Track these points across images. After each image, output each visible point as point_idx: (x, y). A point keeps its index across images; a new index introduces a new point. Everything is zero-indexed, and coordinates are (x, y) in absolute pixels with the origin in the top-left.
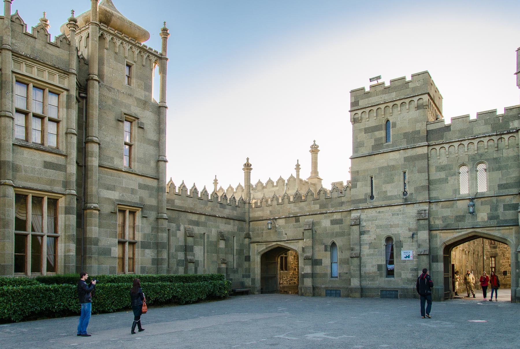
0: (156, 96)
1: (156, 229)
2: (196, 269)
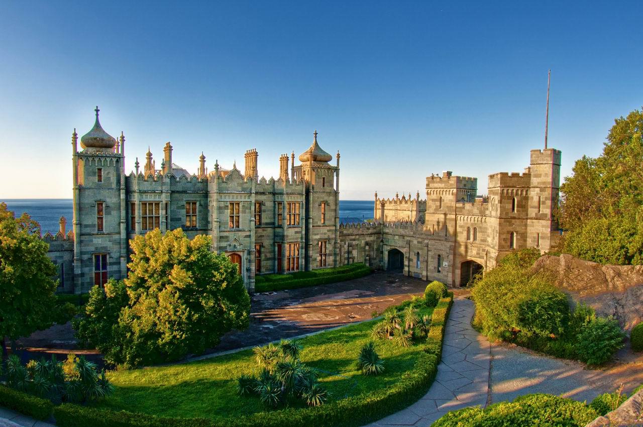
0: (335, 188)
1: (335, 247)
2: (353, 261)
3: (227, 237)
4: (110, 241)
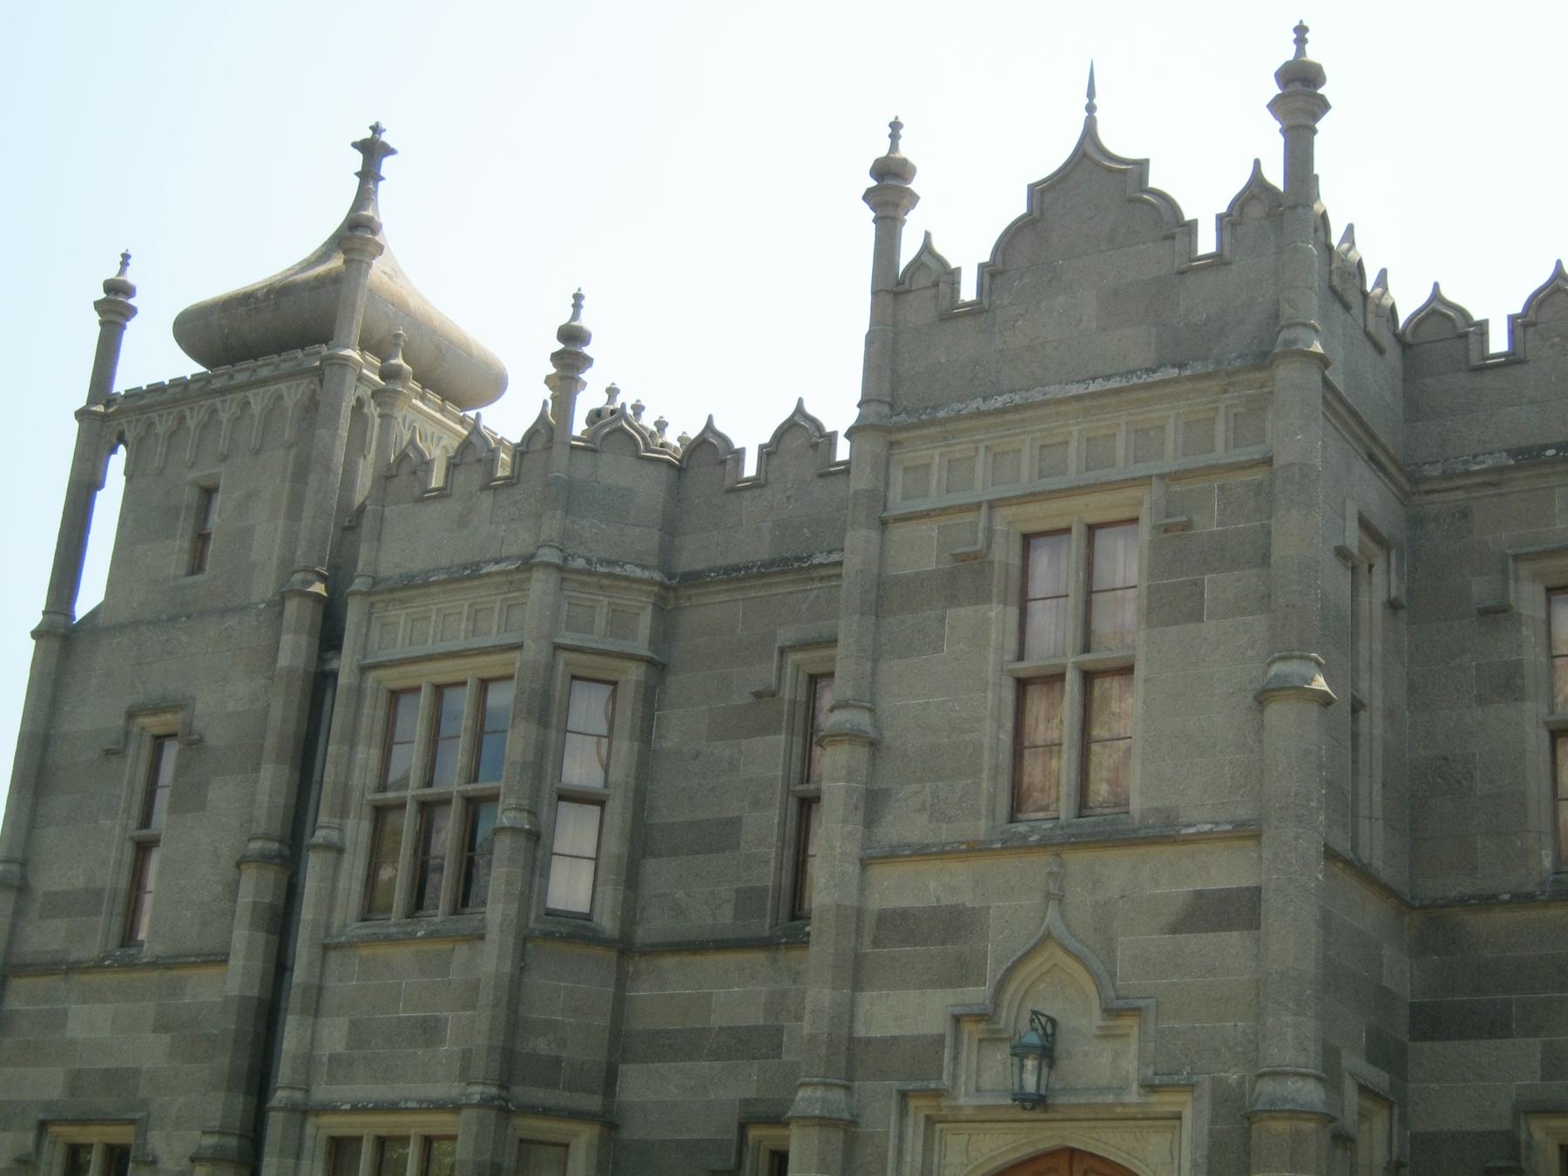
3: (954, 924)
4: (161, 1028)
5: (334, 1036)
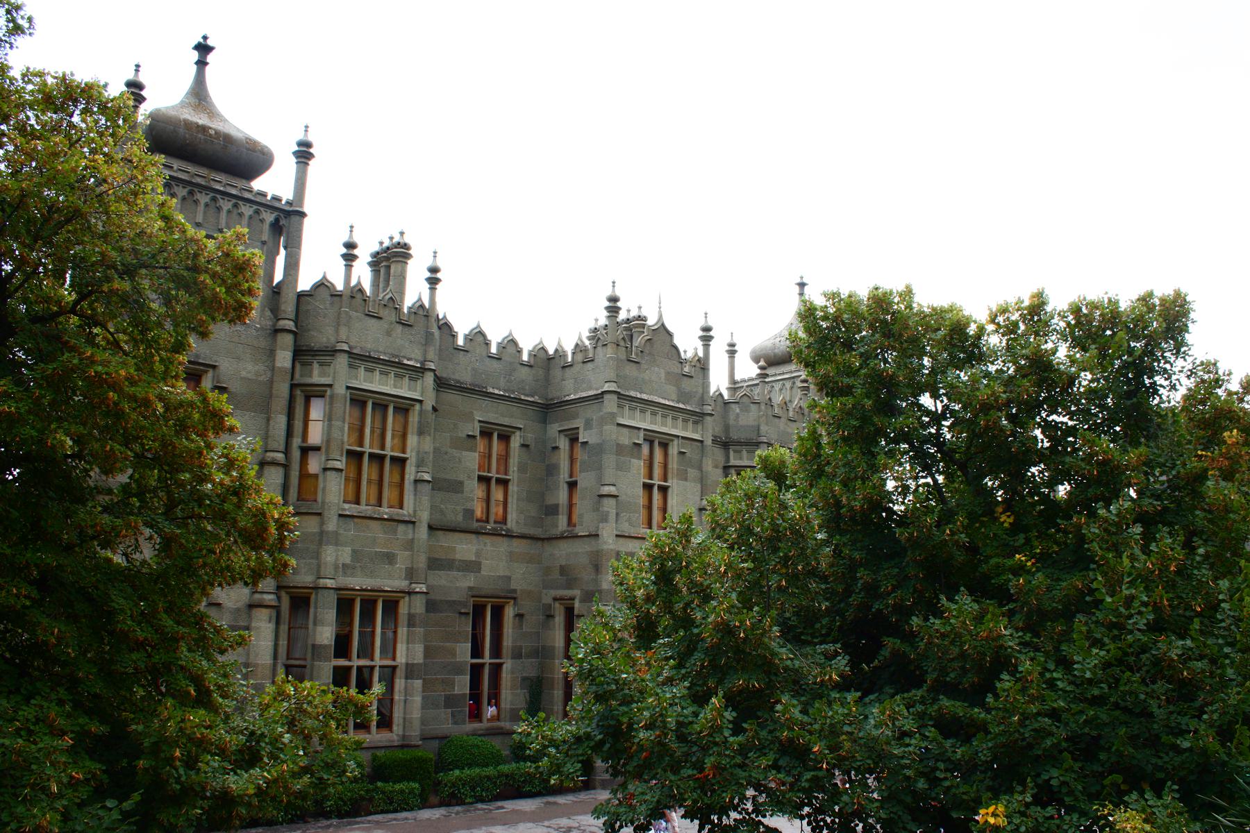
5: (346, 555)
